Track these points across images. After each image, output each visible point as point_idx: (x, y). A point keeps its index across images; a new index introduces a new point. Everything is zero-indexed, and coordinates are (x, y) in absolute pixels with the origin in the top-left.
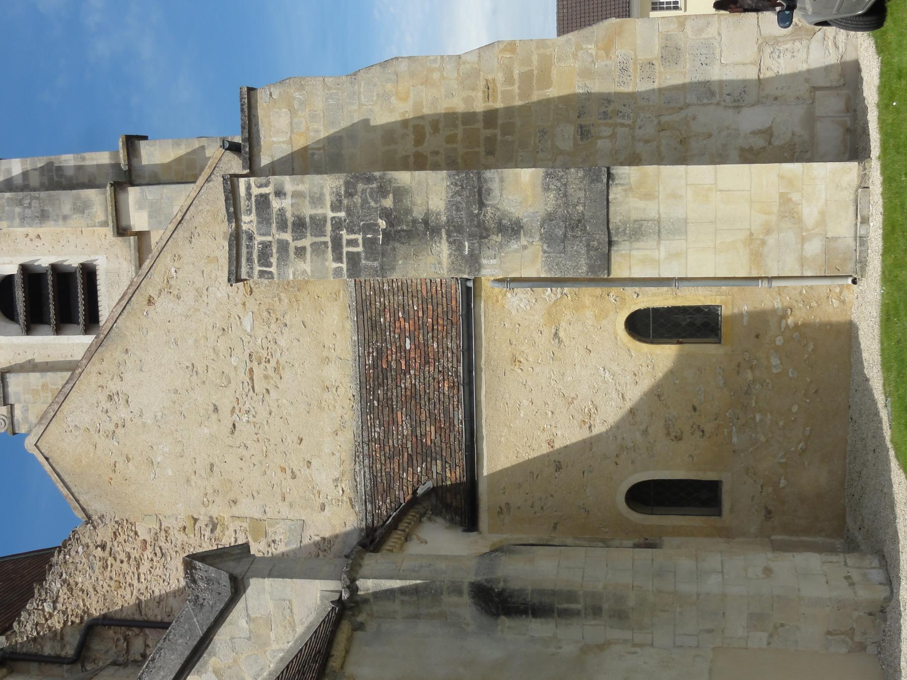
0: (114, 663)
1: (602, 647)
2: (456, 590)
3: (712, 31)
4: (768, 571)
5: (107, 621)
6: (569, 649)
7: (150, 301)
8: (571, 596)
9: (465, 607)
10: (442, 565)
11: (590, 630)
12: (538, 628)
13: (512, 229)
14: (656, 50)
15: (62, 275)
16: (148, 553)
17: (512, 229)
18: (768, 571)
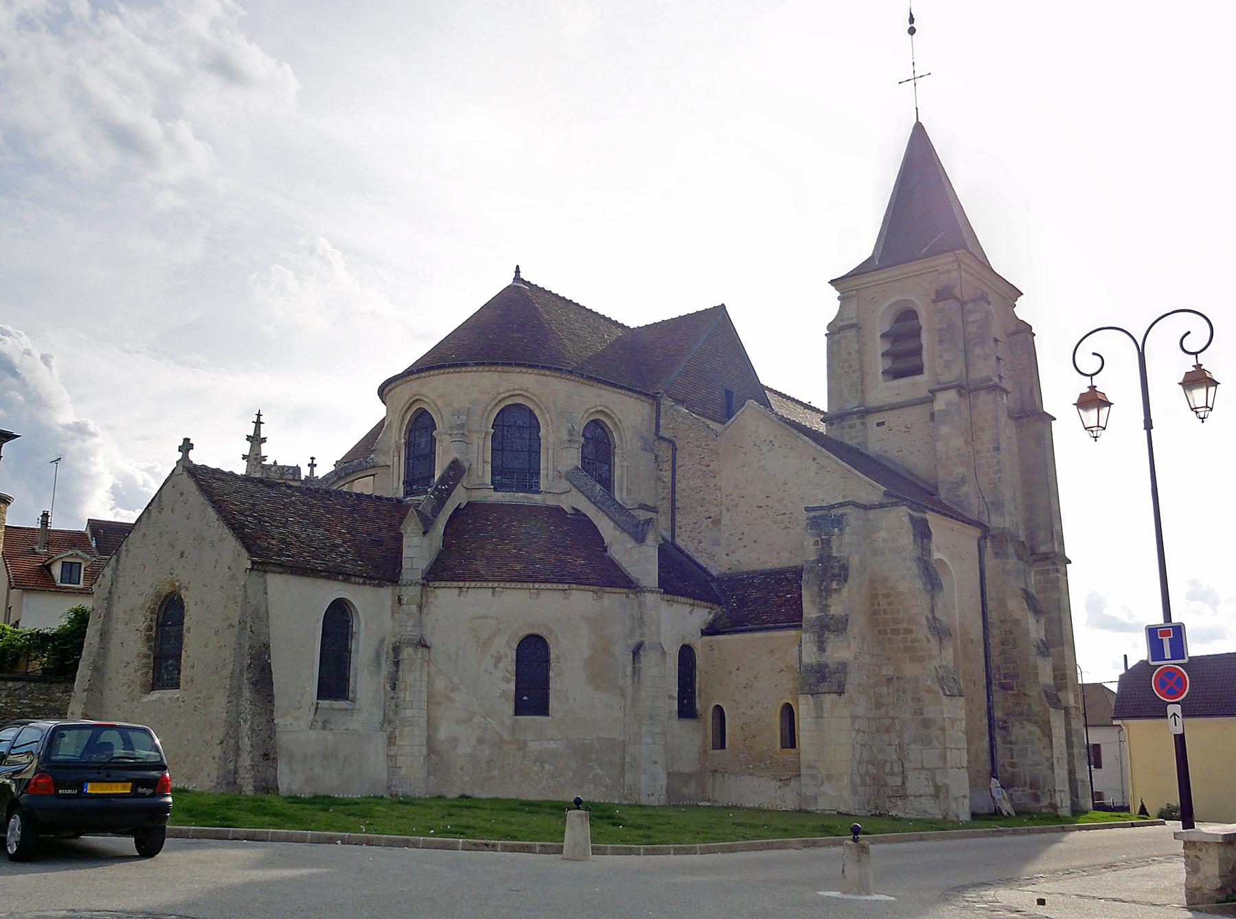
0: (656, 457)
1: (623, 695)
2: (643, 635)
3: (937, 744)
4: (656, 762)
5: (675, 450)
6: (621, 682)
7: (814, 459)
8: (639, 681)
9: (636, 639)
10: (653, 628)
11: (629, 692)
12: (629, 670)
13: (822, 648)
14: (927, 716)
15: (918, 352)
16: (704, 468)
17: (822, 648)
18: (656, 762)
